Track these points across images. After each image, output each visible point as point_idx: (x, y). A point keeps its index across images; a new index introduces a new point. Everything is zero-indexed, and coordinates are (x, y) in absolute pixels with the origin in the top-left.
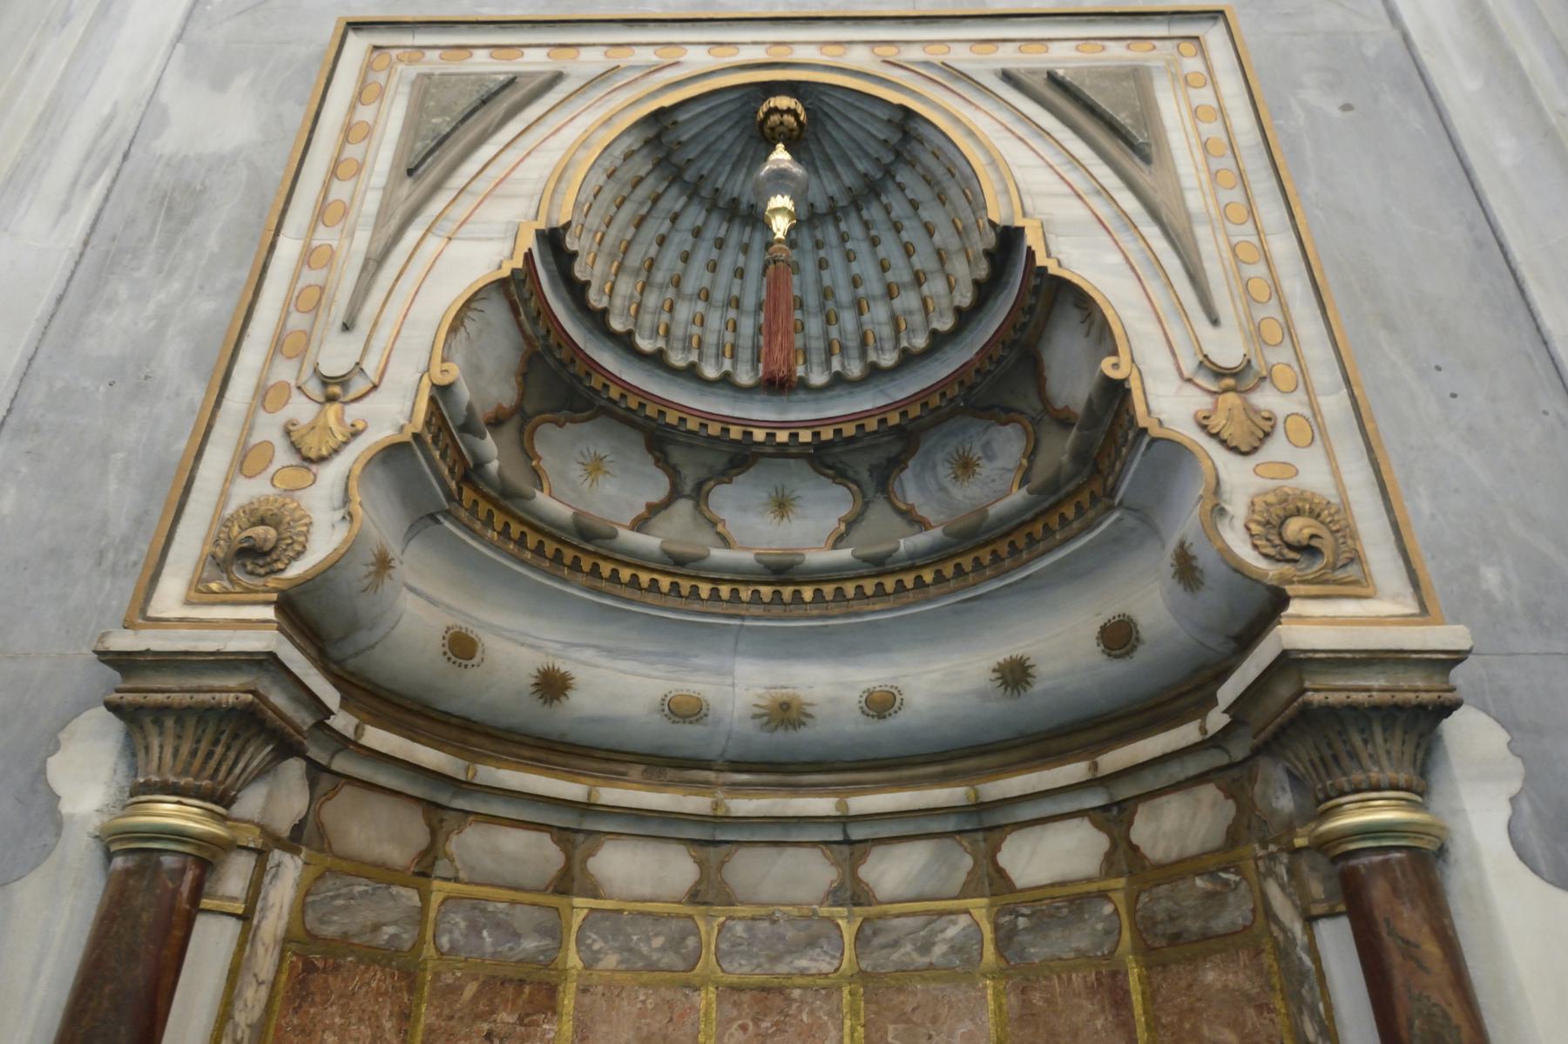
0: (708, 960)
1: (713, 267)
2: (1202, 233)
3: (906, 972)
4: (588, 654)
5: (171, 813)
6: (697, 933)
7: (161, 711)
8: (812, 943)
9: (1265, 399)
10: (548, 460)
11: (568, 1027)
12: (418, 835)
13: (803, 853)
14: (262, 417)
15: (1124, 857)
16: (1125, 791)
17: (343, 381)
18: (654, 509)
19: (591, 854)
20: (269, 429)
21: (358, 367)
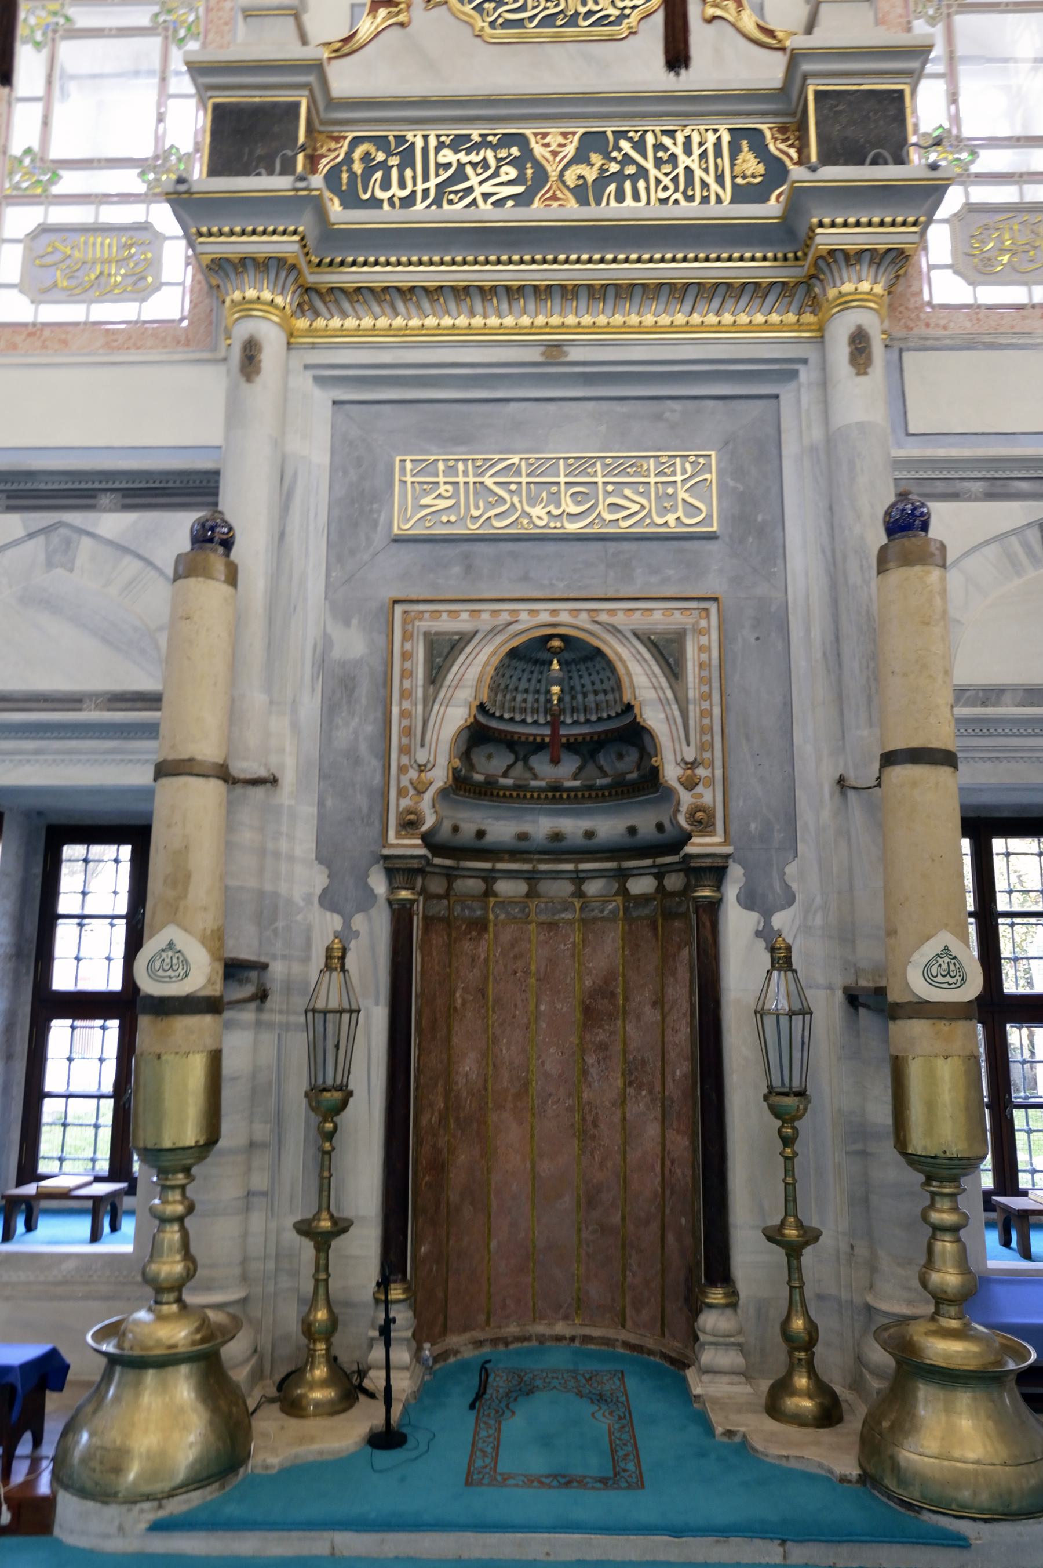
0: (533, 916)
1: (529, 680)
2: (691, 707)
3: (595, 920)
4: (489, 820)
5: (404, 894)
6: (528, 906)
7: (398, 869)
8: (566, 910)
9: (701, 772)
10: (475, 758)
11: (491, 936)
12: (445, 885)
13: (564, 881)
14: (402, 777)
15: (660, 888)
16: (663, 869)
17: (425, 765)
18: (509, 767)
19: (494, 883)
20: (405, 782)
21: (428, 761)
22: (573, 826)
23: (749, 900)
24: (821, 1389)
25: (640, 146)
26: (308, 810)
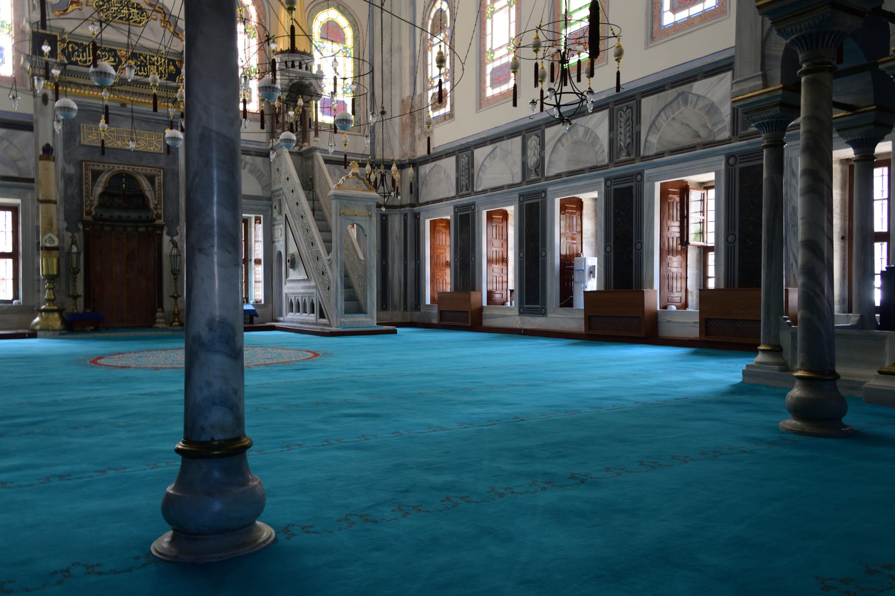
22: (124, 215)
23: (168, 234)
24: (179, 321)
25: (145, 58)
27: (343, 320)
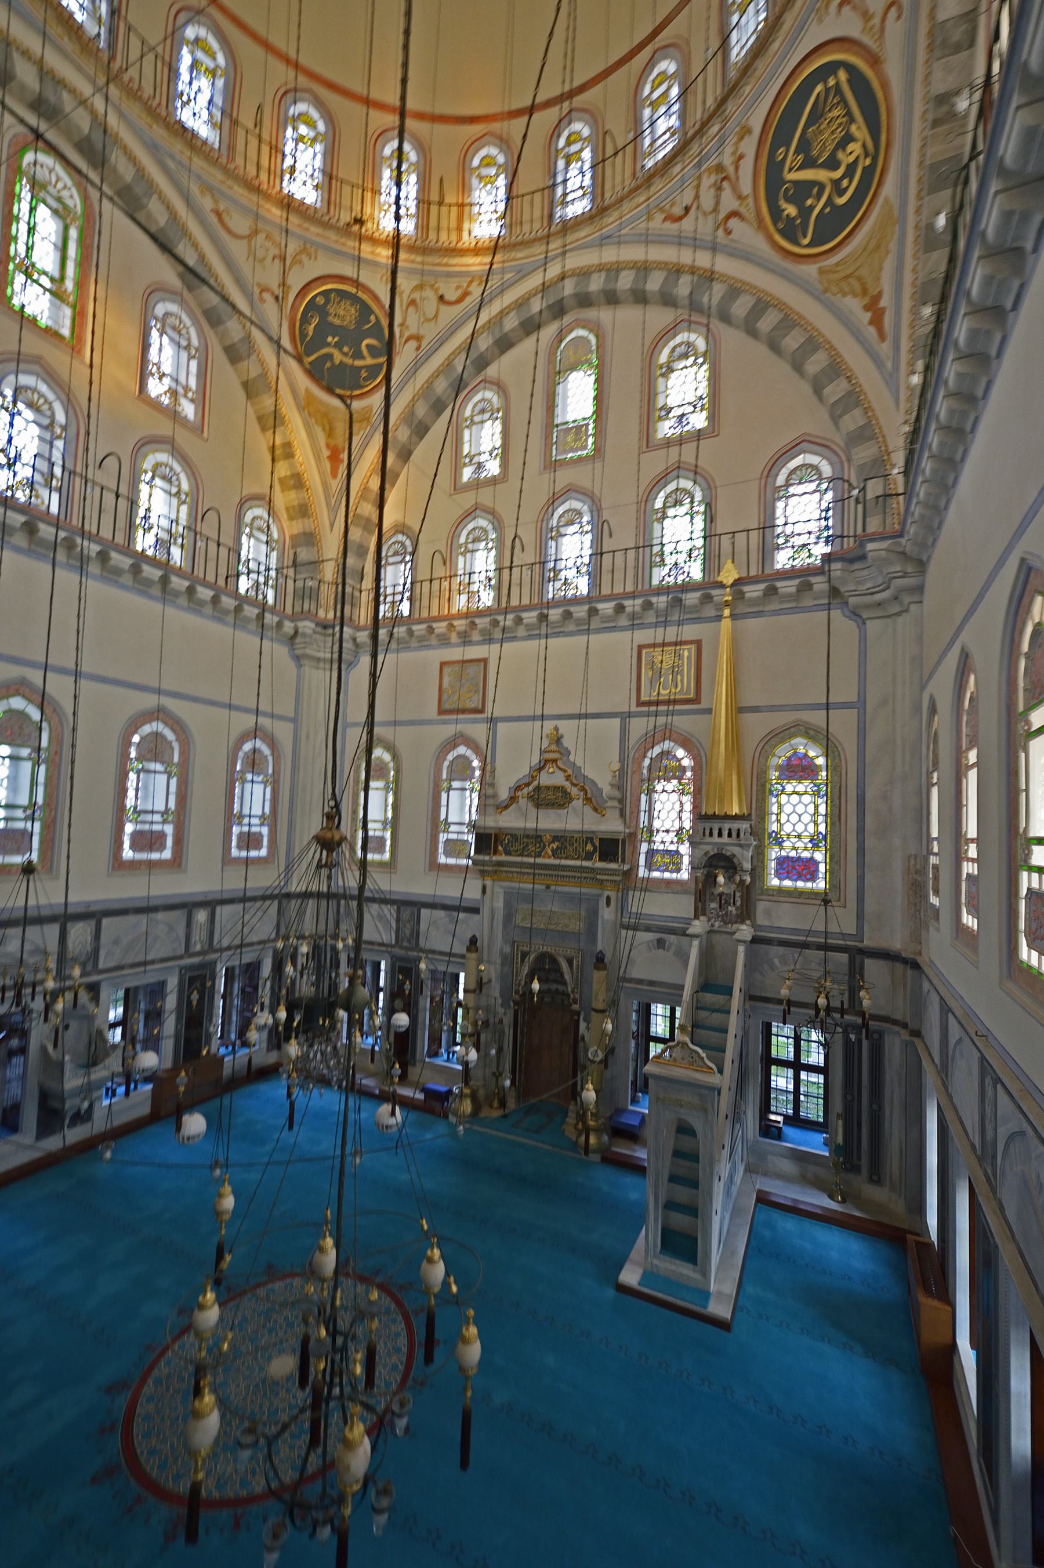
26: (498, 987)
27: (656, 1262)
